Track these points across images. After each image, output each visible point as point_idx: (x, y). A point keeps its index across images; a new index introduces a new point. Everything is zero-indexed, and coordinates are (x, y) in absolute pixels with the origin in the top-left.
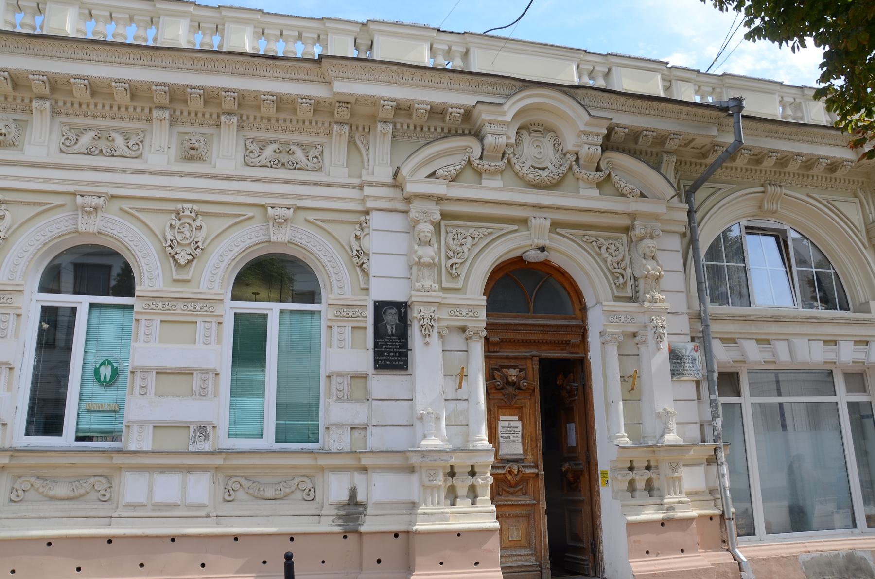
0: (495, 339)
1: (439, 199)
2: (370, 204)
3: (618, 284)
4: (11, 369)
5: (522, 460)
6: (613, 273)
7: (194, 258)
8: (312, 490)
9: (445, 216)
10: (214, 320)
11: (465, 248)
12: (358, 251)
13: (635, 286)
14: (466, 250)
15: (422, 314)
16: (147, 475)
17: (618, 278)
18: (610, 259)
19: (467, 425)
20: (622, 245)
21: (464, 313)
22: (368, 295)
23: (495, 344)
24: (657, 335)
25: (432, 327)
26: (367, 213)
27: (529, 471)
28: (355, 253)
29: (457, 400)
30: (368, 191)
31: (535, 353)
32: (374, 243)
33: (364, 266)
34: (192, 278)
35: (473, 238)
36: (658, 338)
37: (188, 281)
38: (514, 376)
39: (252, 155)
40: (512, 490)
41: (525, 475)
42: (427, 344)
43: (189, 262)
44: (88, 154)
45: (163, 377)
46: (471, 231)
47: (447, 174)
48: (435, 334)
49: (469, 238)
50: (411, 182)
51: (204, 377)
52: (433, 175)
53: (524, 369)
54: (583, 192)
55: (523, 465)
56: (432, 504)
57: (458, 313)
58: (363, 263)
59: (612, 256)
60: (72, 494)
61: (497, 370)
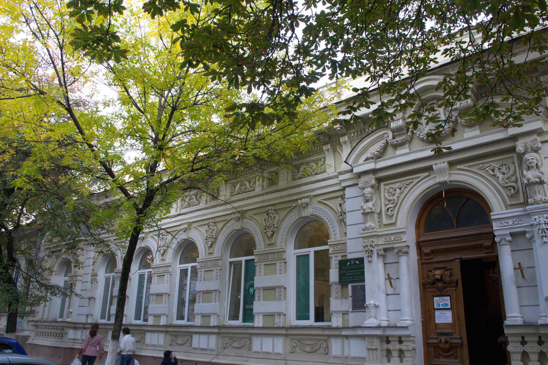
0: (427, 250)
1: (374, 171)
2: (344, 184)
3: (510, 195)
4: (220, 292)
5: (452, 334)
6: (506, 187)
7: (274, 232)
8: (327, 348)
9: (379, 180)
10: (282, 261)
11: (395, 197)
12: (341, 212)
13: (525, 194)
14: (395, 197)
15: (366, 244)
16: (272, 338)
17: (510, 189)
18: (501, 176)
19: (388, 311)
20: (513, 163)
21: (392, 239)
22: (346, 237)
23: (427, 254)
24: (540, 231)
25: (372, 251)
26: (344, 189)
27: (454, 341)
28: (340, 214)
29: (395, 294)
30: (341, 177)
31: (458, 256)
32: (349, 205)
33: (345, 220)
34: (274, 242)
35: (400, 189)
36: (542, 233)
37: (273, 244)
38: (438, 275)
39: (295, 174)
40: (445, 354)
41: (453, 345)
42: (370, 262)
43: (273, 235)
44: (239, 194)
45: (265, 291)
46: (398, 185)
47: (372, 156)
48: (375, 256)
49: (398, 190)
50: (355, 166)
51: (280, 290)
52: (367, 159)
53: (451, 269)
54: (466, 135)
55: (451, 337)
56: (373, 360)
57: (389, 240)
58: (344, 219)
59: (504, 174)
60: (239, 346)
61: (431, 271)
